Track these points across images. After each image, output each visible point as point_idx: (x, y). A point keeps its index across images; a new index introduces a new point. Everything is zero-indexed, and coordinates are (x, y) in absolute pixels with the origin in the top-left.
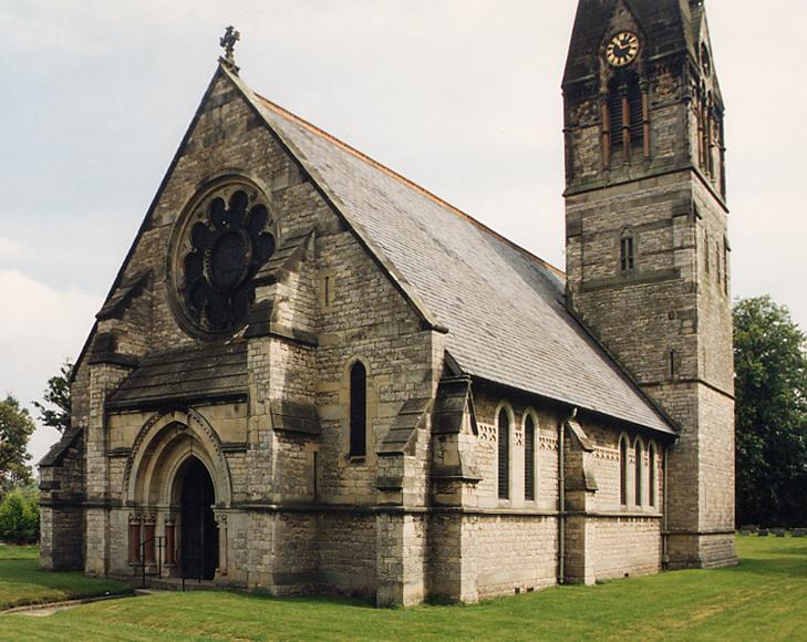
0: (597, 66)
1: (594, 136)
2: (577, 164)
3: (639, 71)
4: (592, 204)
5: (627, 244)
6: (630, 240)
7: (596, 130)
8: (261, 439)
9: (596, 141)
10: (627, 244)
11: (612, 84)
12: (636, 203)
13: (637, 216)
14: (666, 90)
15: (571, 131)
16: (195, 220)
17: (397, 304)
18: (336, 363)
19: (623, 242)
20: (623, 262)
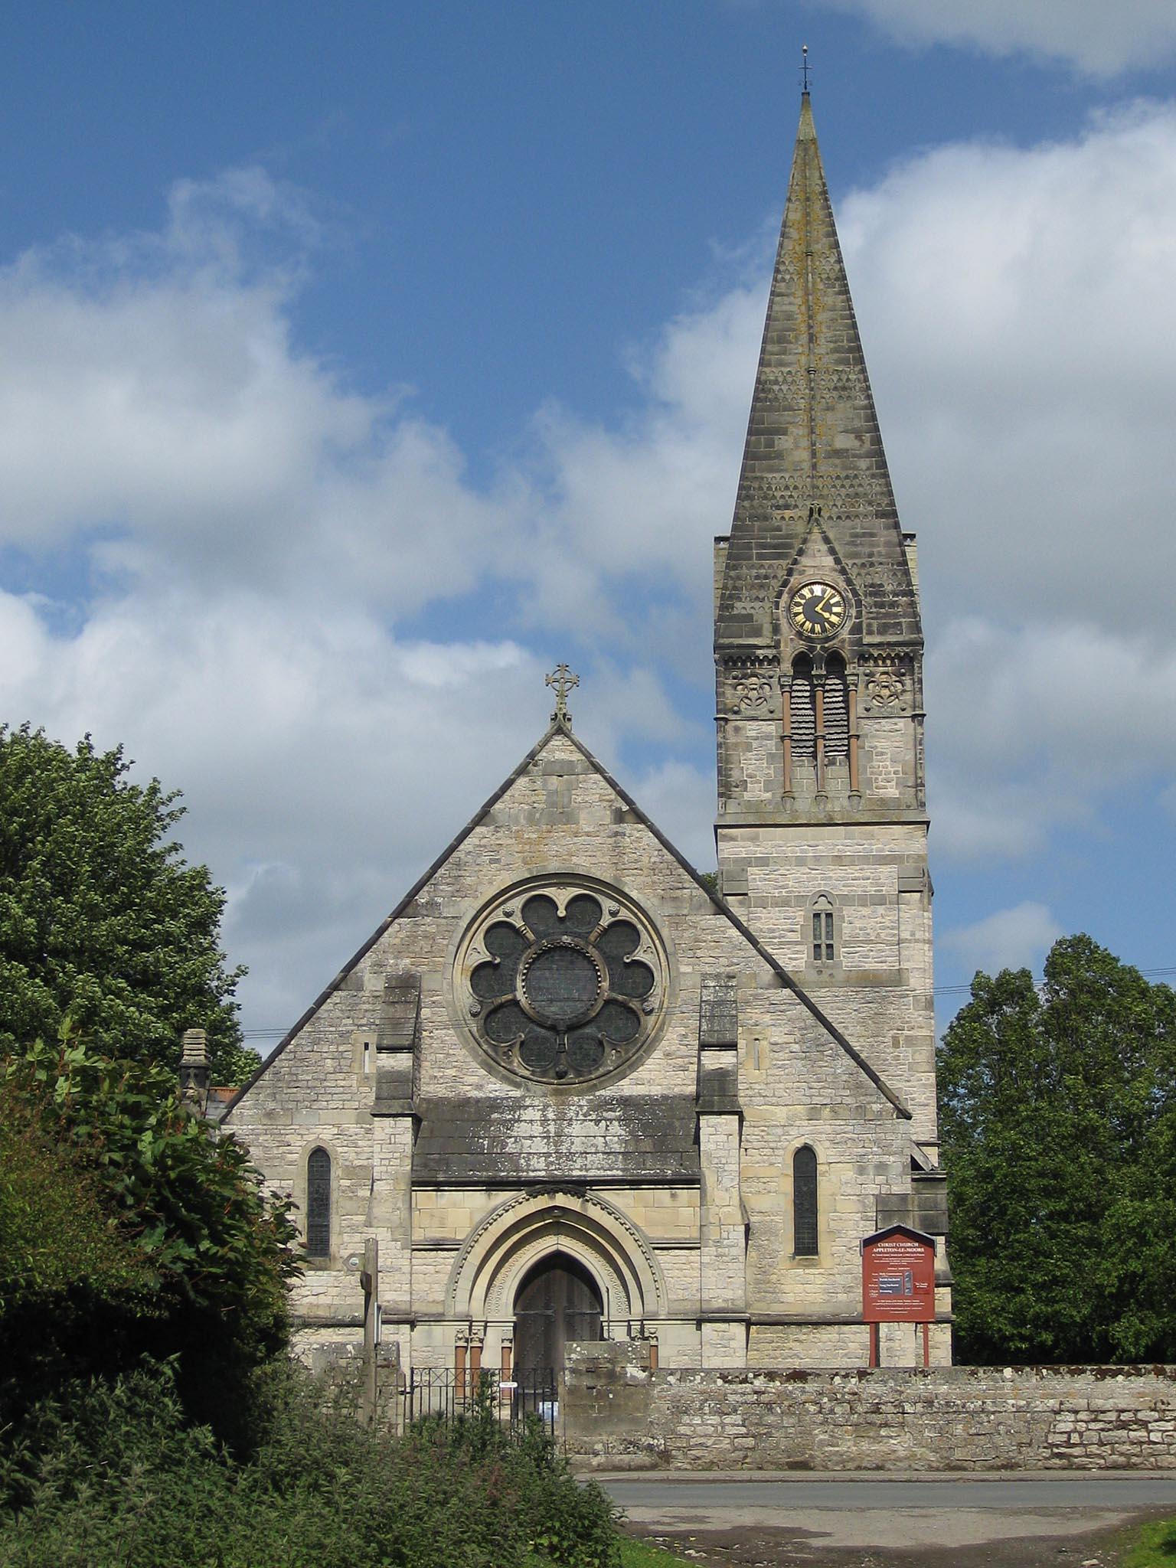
0: (776, 629)
1: (768, 737)
2: (735, 775)
3: (846, 654)
4: (759, 851)
5: (824, 921)
6: (829, 915)
7: (771, 728)
8: (725, 1235)
9: (772, 745)
10: (824, 921)
11: (802, 664)
12: (838, 860)
13: (839, 880)
14: (886, 692)
15: (726, 720)
16: (498, 916)
17: (859, 1086)
18: (772, 1145)
19: (817, 916)
20: (817, 947)
